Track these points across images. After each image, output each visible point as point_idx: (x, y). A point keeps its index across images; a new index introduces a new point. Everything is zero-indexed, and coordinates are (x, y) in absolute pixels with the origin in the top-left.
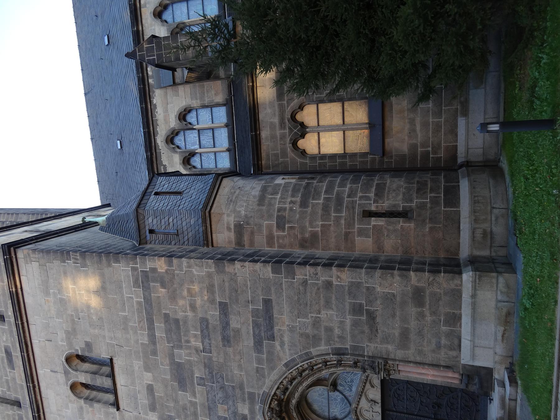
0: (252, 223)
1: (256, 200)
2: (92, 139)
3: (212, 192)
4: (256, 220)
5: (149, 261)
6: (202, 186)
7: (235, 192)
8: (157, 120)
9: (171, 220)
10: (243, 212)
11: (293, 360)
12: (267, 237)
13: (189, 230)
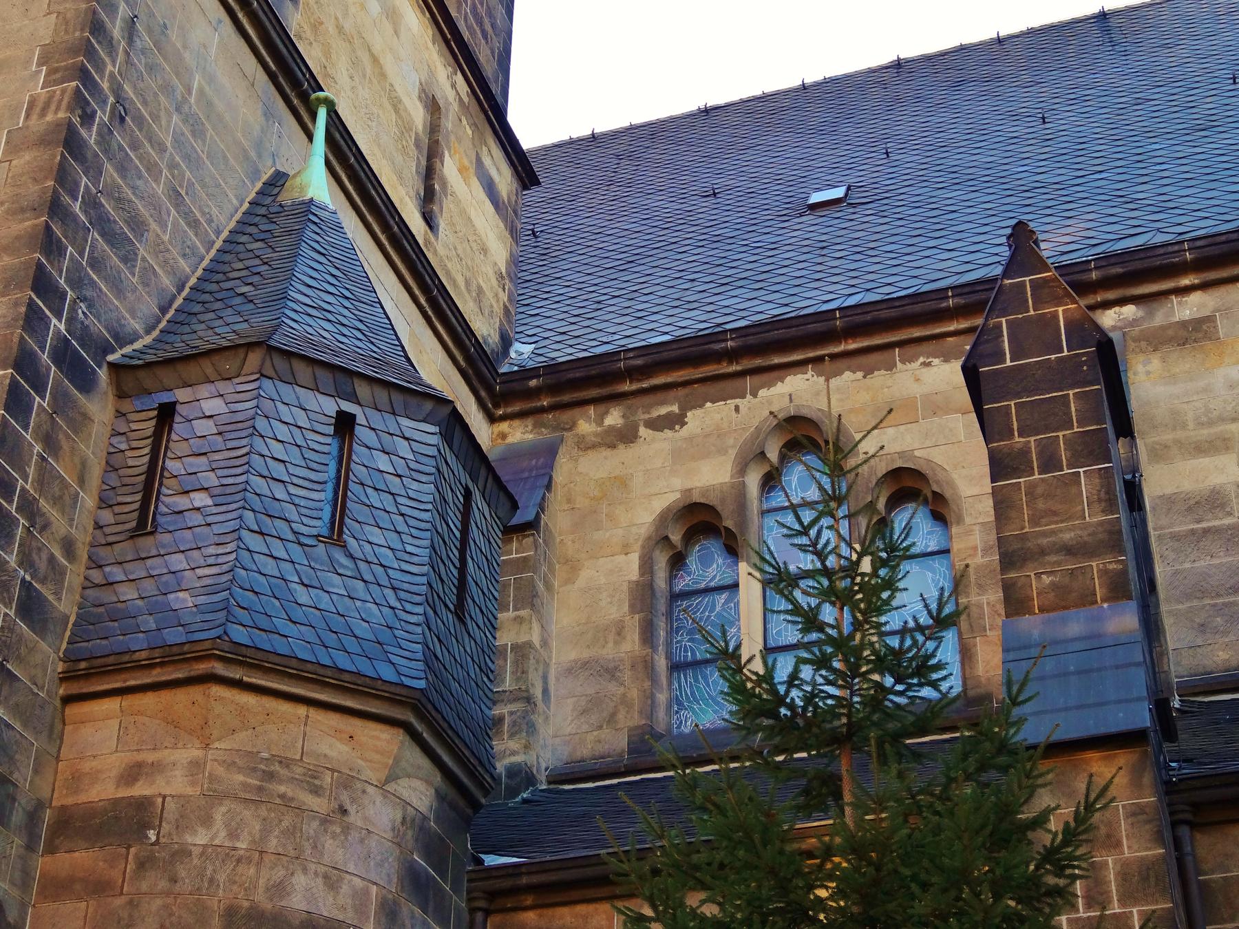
0: (144, 886)
1: (260, 897)
2: (898, 65)
4: (159, 902)
6: (362, 629)
7: (316, 791)
8: (891, 367)
9: (200, 499)
10: (200, 838)
13: (149, 587)
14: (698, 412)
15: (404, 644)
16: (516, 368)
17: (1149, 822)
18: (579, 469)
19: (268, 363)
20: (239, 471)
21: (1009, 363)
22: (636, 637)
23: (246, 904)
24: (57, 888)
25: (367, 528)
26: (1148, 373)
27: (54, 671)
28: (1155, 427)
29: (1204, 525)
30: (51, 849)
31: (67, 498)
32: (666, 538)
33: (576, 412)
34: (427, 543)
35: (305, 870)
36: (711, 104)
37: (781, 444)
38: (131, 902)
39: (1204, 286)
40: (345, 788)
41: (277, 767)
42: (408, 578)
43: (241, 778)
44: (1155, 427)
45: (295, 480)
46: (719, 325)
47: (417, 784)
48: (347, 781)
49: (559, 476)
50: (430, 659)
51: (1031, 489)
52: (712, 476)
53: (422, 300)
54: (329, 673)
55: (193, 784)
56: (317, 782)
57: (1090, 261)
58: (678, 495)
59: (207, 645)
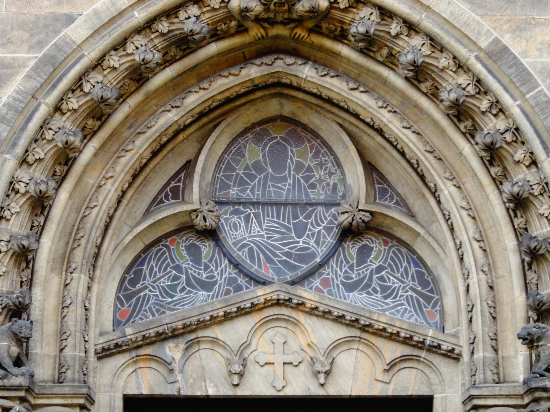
11: (525, 78)
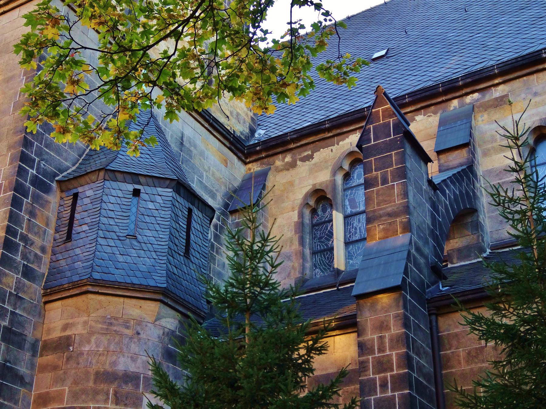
0: (69, 366)
1: (107, 367)
3: (127, 289)
4: (73, 371)
5: (5, 212)
6: (143, 268)
7: (127, 327)
9: (85, 228)
10: (87, 348)
12: (48, 393)
14: (318, 153)
15: (159, 271)
16: (257, 141)
17: (400, 320)
18: (277, 180)
19: (107, 176)
20: (97, 216)
21: (372, 143)
22: (297, 244)
23: (102, 370)
24: (44, 368)
25: (145, 231)
26: (483, 120)
27: (40, 293)
28: (485, 142)
29: (503, 180)
30: (41, 356)
31: (41, 233)
32: (308, 204)
33: (275, 157)
34: (168, 233)
35: (124, 356)
36: (350, 15)
37: (349, 162)
38: (64, 372)
39: (504, 82)
40: (139, 325)
41: (113, 321)
42: (161, 247)
43: (101, 326)
44: (485, 142)
45: (118, 217)
46: (328, 117)
47: (171, 320)
48: (139, 322)
49: (269, 184)
50: (169, 275)
51: (378, 191)
52: (323, 177)
53: (206, 125)
54: (130, 286)
55: (84, 329)
56: (128, 324)
57: (458, 78)
58: (311, 187)
59: (85, 281)
